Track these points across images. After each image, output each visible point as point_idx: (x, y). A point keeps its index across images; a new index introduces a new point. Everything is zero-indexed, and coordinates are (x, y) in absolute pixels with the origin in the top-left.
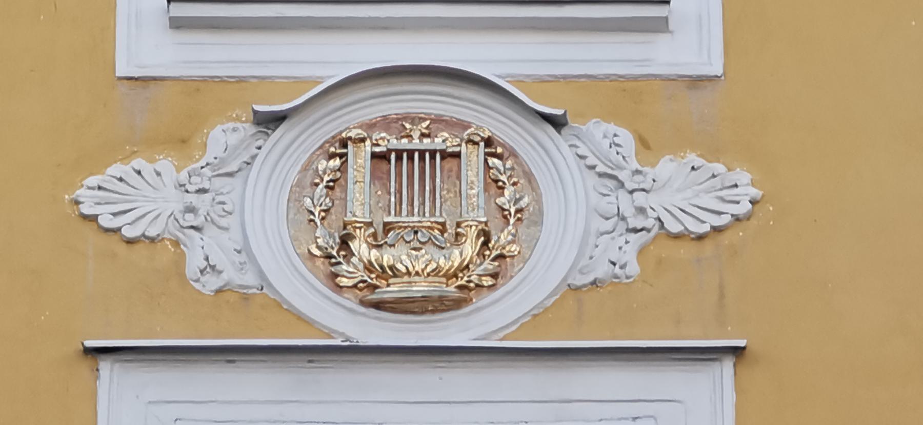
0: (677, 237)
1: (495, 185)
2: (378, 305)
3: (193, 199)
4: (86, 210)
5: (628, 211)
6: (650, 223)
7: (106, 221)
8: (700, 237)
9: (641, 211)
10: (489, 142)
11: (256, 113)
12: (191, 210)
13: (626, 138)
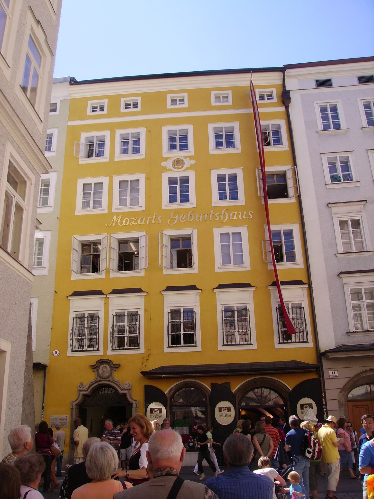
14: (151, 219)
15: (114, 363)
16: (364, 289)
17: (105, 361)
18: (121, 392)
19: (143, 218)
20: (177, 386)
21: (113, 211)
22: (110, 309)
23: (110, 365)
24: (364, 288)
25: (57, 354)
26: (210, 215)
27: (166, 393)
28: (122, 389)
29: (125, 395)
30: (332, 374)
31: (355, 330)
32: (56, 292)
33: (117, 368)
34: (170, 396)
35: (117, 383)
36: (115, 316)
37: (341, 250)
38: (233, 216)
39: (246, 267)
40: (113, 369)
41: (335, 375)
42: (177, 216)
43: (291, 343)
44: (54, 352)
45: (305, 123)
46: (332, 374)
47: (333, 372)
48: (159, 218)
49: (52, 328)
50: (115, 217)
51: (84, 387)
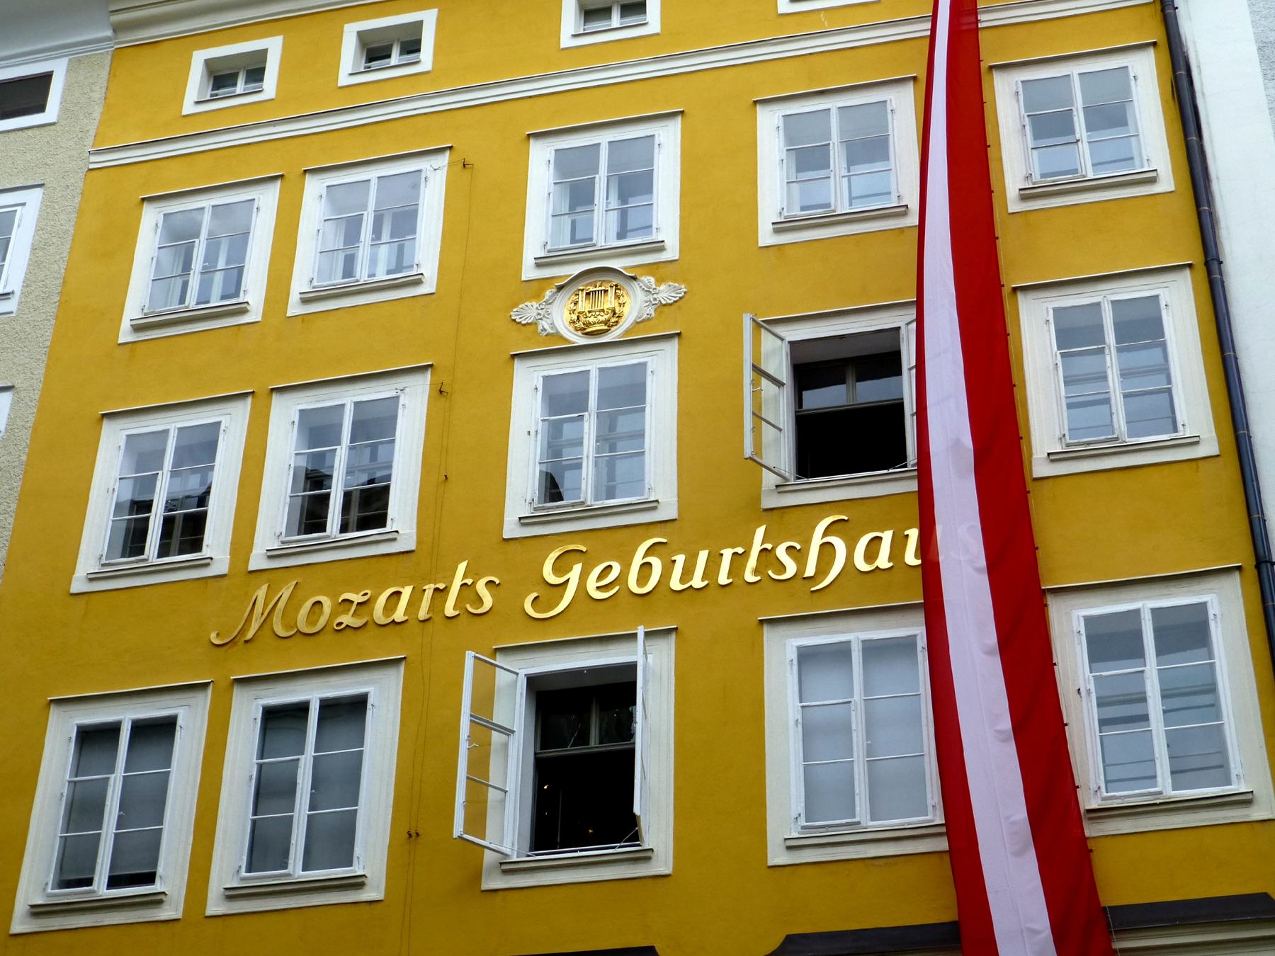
0: (665, 305)
1: (618, 297)
2: (587, 334)
3: (540, 312)
4: (513, 318)
5: (652, 299)
6: (657, 302)
7: (518, 320)
8: (671, 304)
9: (655, 299)
10: (616, 286)
11: (556, 286)
12: (539, 314)
13: (652, 279)
14: (440, 593)
19: (398, 594)
21: (257, 561)
26: (746, 554)
38: (871, 555)
42: (577, 568)
48: (481, 587)
50: (261, 593)
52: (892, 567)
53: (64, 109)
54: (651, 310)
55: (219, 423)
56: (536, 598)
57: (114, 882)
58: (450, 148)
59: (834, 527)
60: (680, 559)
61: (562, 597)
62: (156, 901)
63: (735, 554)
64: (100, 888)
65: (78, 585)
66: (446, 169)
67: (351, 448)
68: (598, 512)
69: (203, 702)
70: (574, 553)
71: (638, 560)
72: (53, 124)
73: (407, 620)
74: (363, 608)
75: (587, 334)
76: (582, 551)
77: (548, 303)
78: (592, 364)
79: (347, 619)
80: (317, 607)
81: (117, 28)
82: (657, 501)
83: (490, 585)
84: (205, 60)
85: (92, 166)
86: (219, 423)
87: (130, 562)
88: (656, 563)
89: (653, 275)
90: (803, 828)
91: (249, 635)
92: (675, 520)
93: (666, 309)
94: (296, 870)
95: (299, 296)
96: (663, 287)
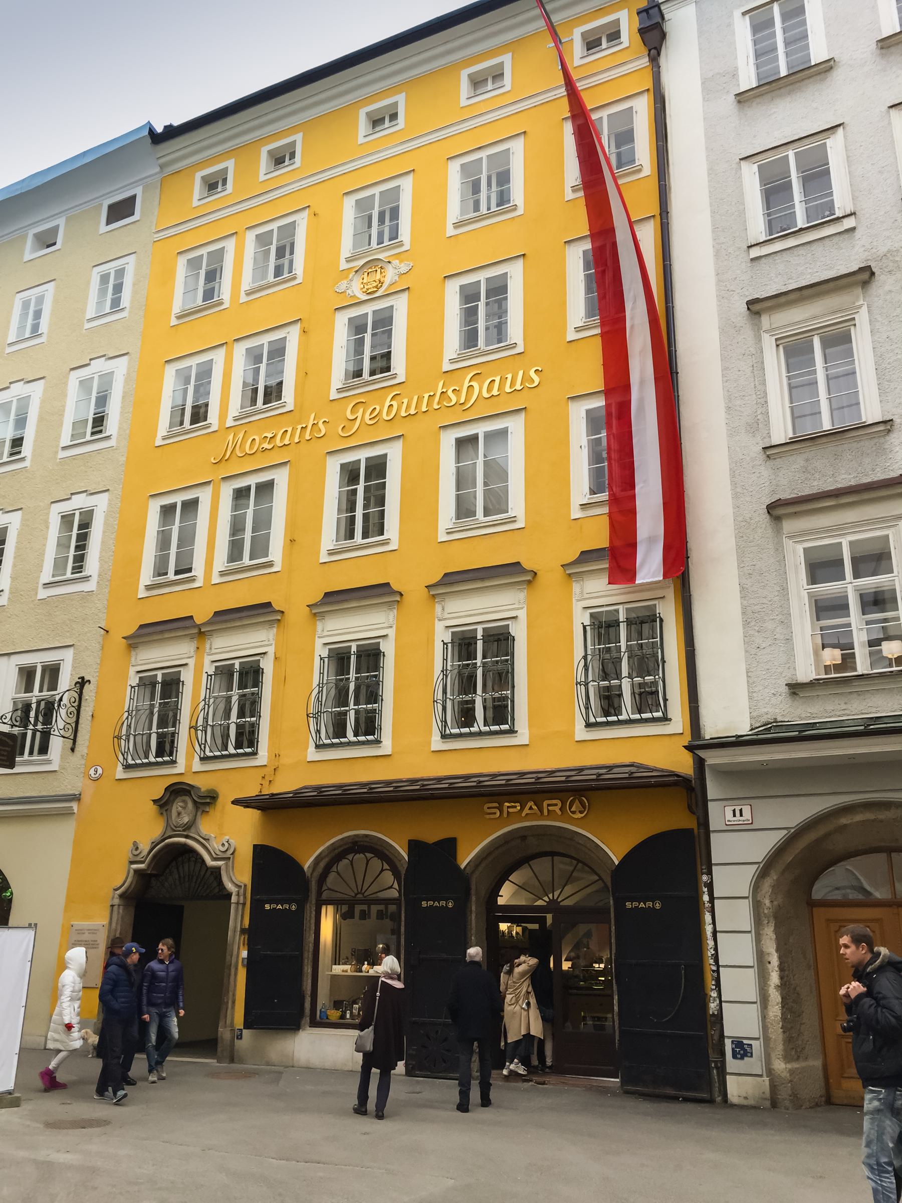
1: (381, 273)
2: (367, 294)
15: (203, 790)
16: (851, 543)
17: (181, 787)
18: (210, 862)
19: (286, 431)
20: (335, 849)
21: (230, 423)
22: (207, 660)
23: (193, 799)
24: (851, 543)
25: (96, 776)
27: (306, 867)
28: (215, 856)
29: (217, 871)
30: (734, 816)
31: (816, 676)
32: (107, 632)
33: (208, 804)
34: (317, 874)
35: (204, 841)
36: (213, 676)
37: (781, 431)
39: (513, 520)
40: (200, 806)
41: (741, 818)
42: (361, 410)
43: (620, 722)
44: (92, 772)
45: (703, 83)
46: (734, 816)
47: (738, 809)
48: (320, 424)
49: (92, 715)
50: (231, 437)
51: (140, 853)
52: (499, 395)
53: (142, 212)
54: (397, 278)
55: (212, 360)
56: (344, 426)
57: (177, 573)
58: (309, 206)
59: (477, 376)
60: (406, 401)
61: (355, 424)
62: (192, 580)
63: (430, 395)
64: (171, 576)
65: (159, 442)
66: (306, 219)
67: (267, 364)
68: (371, 382)
69: (209, 490)
70: (358, 405)
71: (387, 404)
72: (138, 221)
73: (290, 444)
74: (273, 439)
75: (367, 294)
76: (363, 402)
77: (351, 280)
78: (369, 309)
79: (266, 446)
80: (253, 442)
81: (162, 167)
82: (396, 374)
83: (325, 423)
84: (202, 177)
85: (155, 240)
86: (212, 360)
87: (177, 429)
88: (394, 403)
89: (397, 259)
90: (454, 523)
91: (226, 458)
92: (403, 382)
93: (404, 275)
94: (246, 561)
95: (244, 293)
96: (402, 265)
